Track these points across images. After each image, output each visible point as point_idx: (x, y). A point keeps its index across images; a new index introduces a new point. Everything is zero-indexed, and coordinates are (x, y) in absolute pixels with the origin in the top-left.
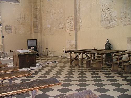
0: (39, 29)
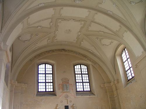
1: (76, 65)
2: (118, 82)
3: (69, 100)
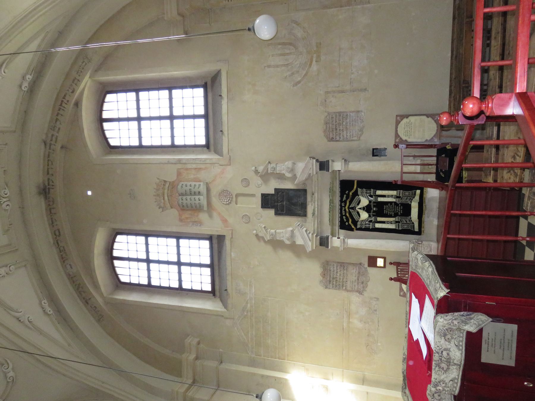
1: (106, 139)
3: (238, 188)
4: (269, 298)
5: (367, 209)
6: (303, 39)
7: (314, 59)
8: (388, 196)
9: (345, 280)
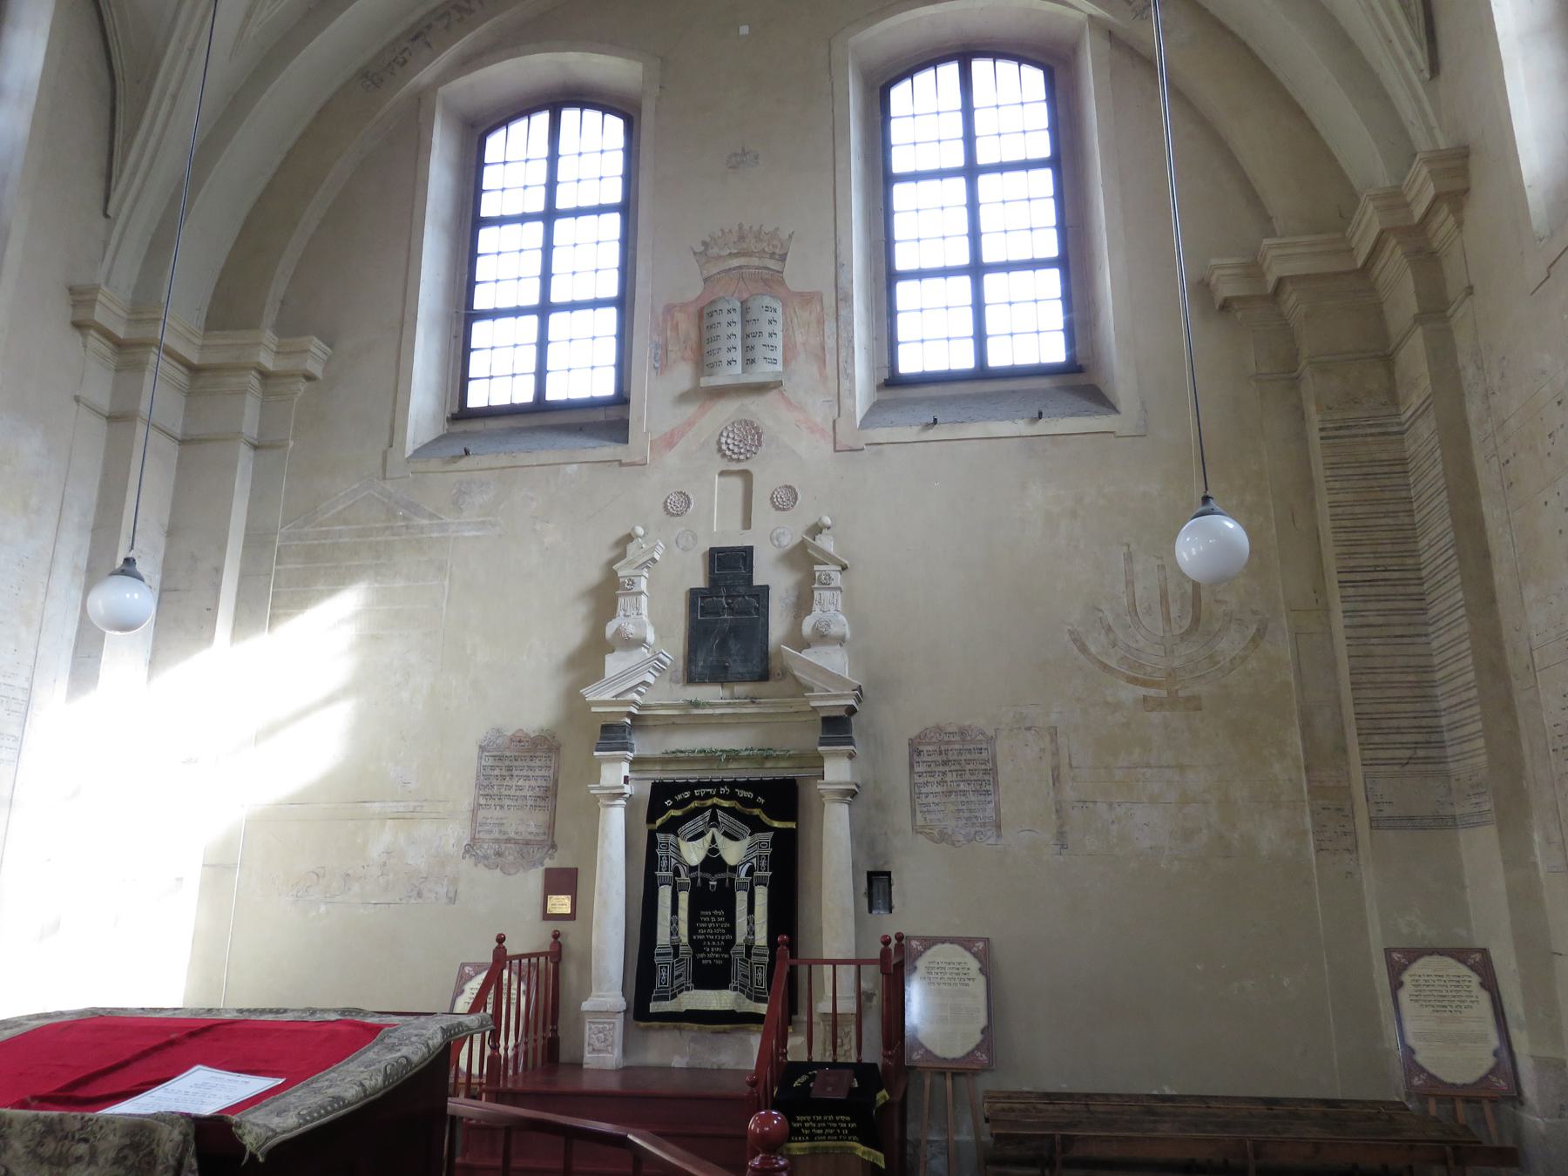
0: (1470, 755)
2: (1455, 196)
4: (446, 583)
5: (713, 861)
6: (1211, 657)
7: (1152, 692)
8: (752, 921)
9: (507, 802)
